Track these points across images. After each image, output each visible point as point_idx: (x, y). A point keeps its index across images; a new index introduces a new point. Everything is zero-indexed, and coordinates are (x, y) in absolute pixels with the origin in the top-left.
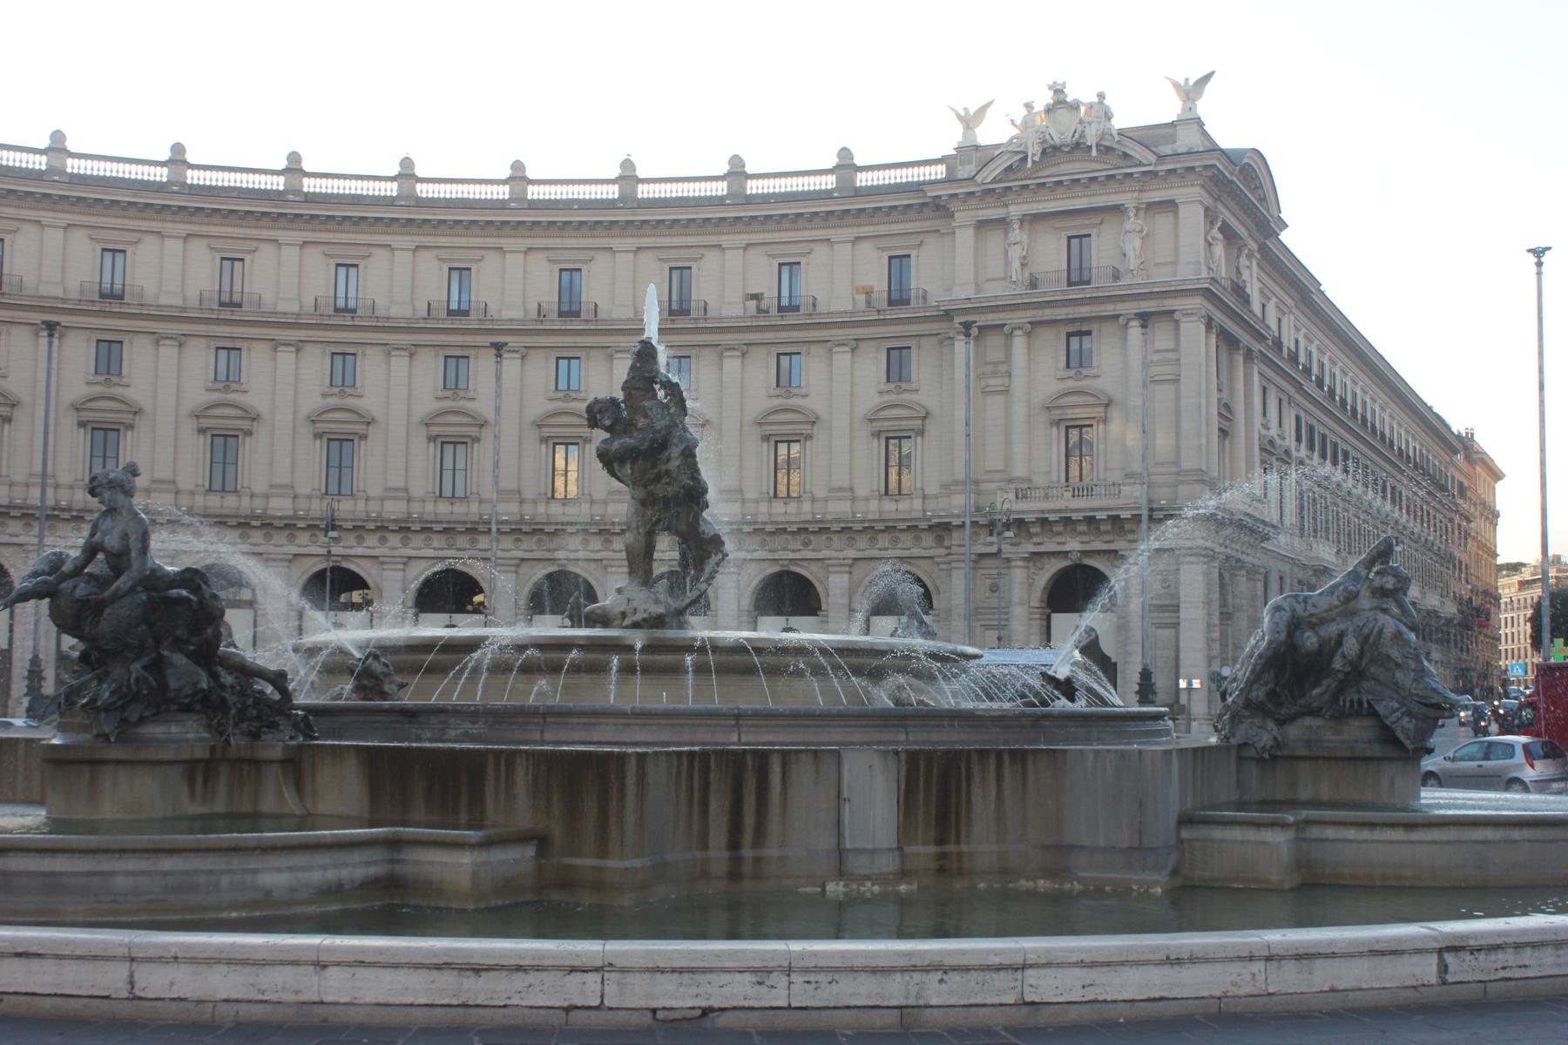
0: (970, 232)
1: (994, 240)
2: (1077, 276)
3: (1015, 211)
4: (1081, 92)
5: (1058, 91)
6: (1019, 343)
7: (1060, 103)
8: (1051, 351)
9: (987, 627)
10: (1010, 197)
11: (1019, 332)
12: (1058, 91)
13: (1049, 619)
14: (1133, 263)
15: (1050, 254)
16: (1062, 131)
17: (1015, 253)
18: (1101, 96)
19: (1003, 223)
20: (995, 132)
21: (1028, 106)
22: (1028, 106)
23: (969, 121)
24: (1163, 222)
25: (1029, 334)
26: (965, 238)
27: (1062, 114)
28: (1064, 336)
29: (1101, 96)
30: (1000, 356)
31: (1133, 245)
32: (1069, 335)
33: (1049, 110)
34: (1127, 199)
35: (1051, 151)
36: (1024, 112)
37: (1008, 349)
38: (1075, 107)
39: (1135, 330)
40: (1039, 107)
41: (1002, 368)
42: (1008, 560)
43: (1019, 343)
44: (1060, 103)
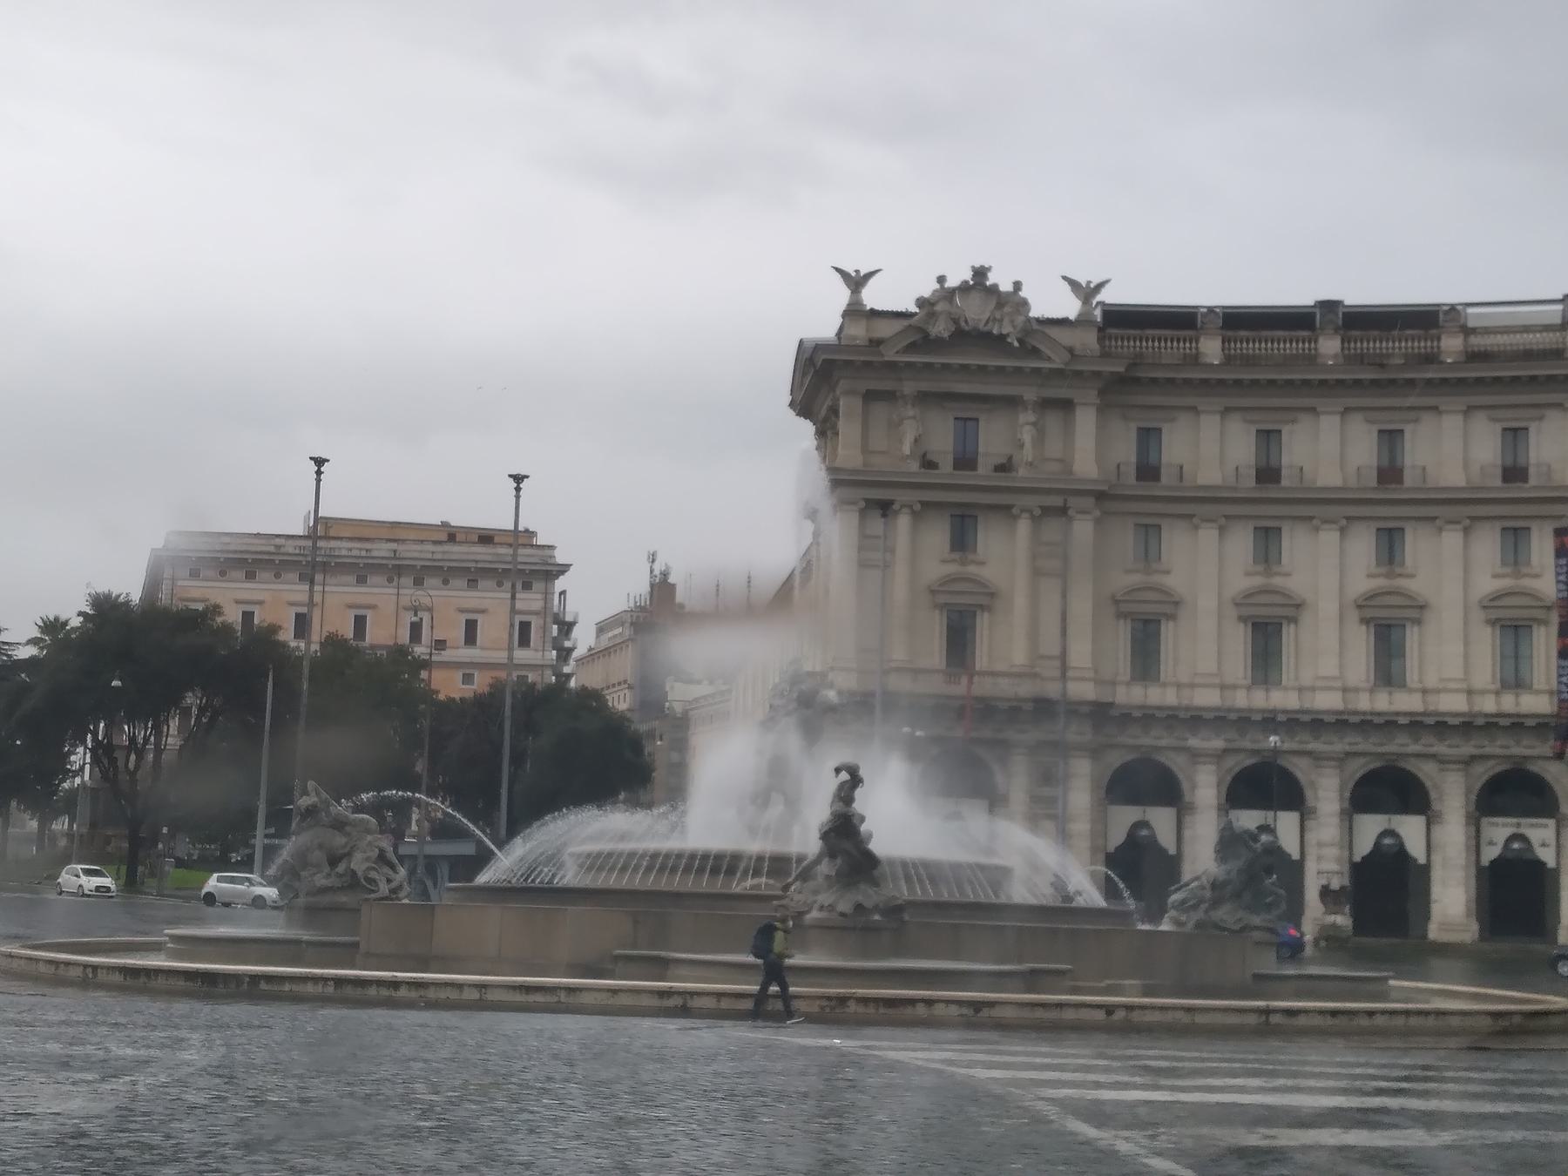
1: (880, 411)
2: (965, 461)
3: (909, 387)
4: (1001, 279)
5: (980, 273)
8: (937, 536)
12: (980, 273)
14: (1028, 453)
15: (942, 437)
16: (975, 312)
17: (909, 433)
18: (1018, 286)
21: (941, 280)
22: (941, 280)
23: (856, 282)
24: (1053, 420)
27: (975, 299)
29: (1018, 286)
31: (1027, 435)
33: (964, 288)
34: (1030, 394)
39: (1023, 527)
40: (952, 282)
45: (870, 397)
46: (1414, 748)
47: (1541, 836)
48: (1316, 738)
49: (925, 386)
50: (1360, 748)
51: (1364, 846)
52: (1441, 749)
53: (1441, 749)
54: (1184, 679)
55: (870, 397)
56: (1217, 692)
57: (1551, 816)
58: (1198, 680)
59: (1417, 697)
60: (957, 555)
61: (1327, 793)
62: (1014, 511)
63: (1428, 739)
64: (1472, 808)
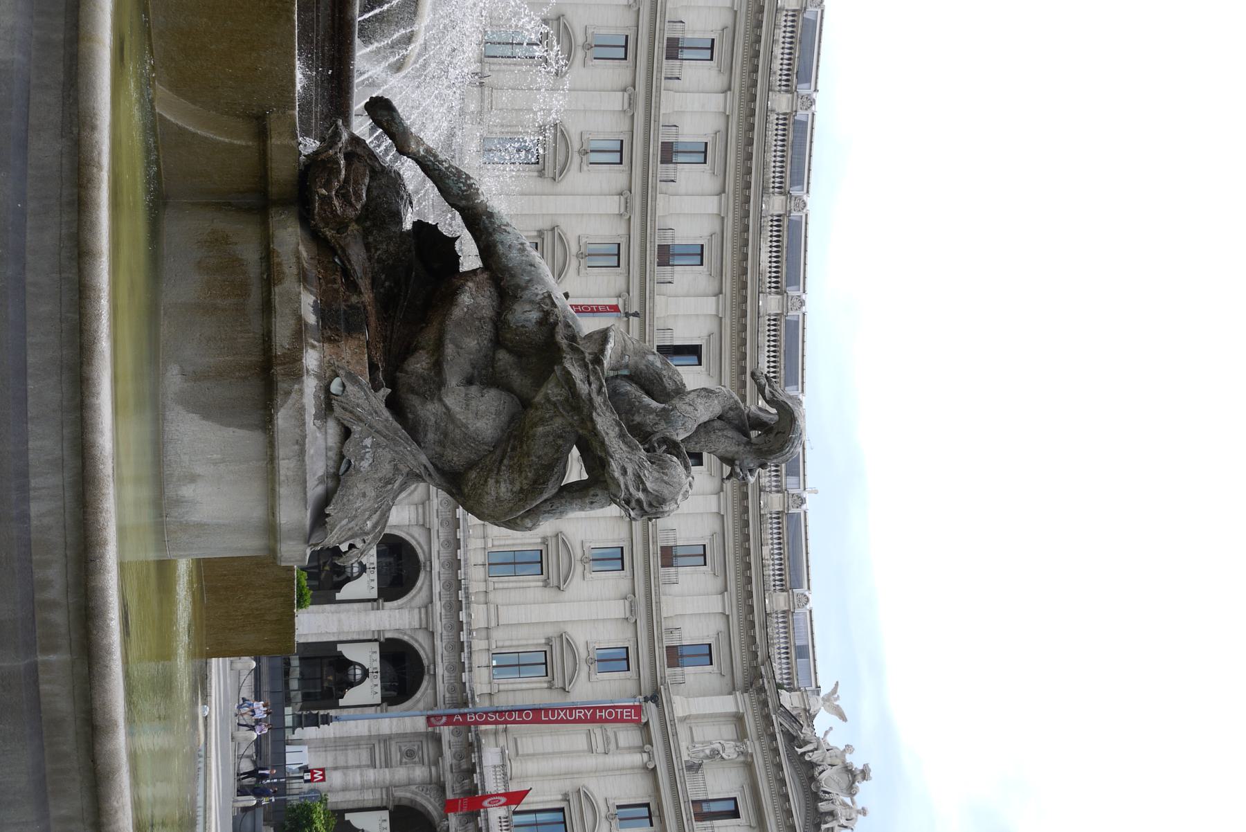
0: (732, 709)
1: (728, 731)
3: (754, 747)
5: (865, 774)
6: (637, 759)
7: (854, 776)
8: (633, 790)
9: (372, 749)
10: (766, 740)
11: (645, 756)
13: (384, 808)
16: (829, 779)
18: (864, 812)
19: (742, 735)
20: (823, 722)
21: (849, 748)
25: (645, 767)
26: (727, 704)
27: (845, 779)
28: (645, 801)
29: (864, 812)
30: (622, 743)
32: (647, 805)
33: (848, 770)
35: (808, 772)
36: (842, 748)
37: (631, 749)
38: (851, 790)
40: (849, 758)
41: (612, 746)
42: (436, 763)
43: (637, 759)
44: (854, 776)
45: (738, 719)
46: (437, 587)
47: (367, 691)
48: (443, 565)
49: (759, 762)
50: (438, 643)
51: (350, 652)
52: (438, 606)
53: (438, 606)
54: (491, 596)
55: (738, 719)
56: (483, 624)
57: (384, 699)
58: (492, 607)
59: (482, 587)
60: (613, 810)
61: (397, 619)
62: (647, 747)
63: (445, 554)
64: (389, 635)
